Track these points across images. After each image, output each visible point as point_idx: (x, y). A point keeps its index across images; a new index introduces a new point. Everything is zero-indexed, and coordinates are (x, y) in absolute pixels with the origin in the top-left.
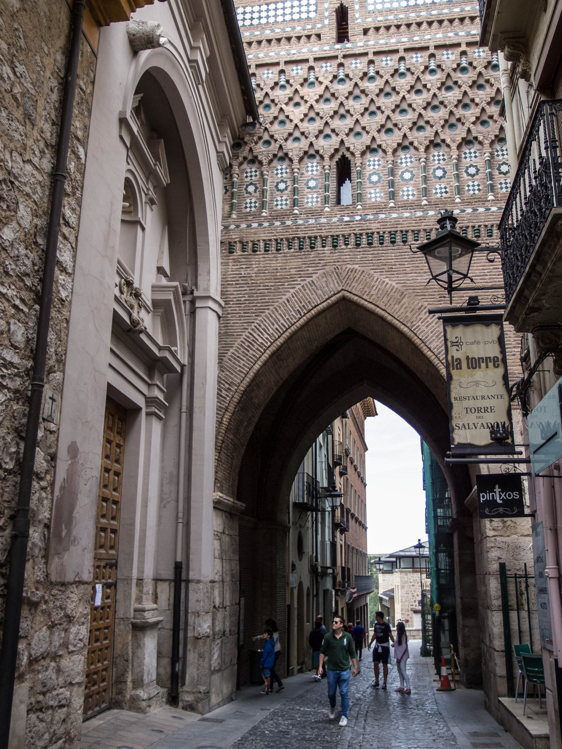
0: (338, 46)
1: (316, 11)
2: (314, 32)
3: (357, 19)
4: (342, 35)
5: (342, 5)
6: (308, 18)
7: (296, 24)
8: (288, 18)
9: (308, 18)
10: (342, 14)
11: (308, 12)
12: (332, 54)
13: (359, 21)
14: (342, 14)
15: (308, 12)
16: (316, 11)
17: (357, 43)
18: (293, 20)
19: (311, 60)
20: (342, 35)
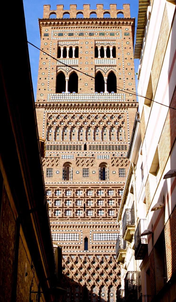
0: (85, 251)
1: (79, 238)
2: (78, 245)
3: (91, 243)
4: (86, 248)
5: (86, 237)
6: (76, 240)
7: (73, 242)
8: (70, 239)
9: (76, 240)
10: (86, 240)
12: (83, 253)
13: (91, 243)
14: (86, 240)
15: (76, 238)
16: (79, 238)
17: (90, 251)
18: (72, 240)
19: (77, 255)
20: (86, 248)
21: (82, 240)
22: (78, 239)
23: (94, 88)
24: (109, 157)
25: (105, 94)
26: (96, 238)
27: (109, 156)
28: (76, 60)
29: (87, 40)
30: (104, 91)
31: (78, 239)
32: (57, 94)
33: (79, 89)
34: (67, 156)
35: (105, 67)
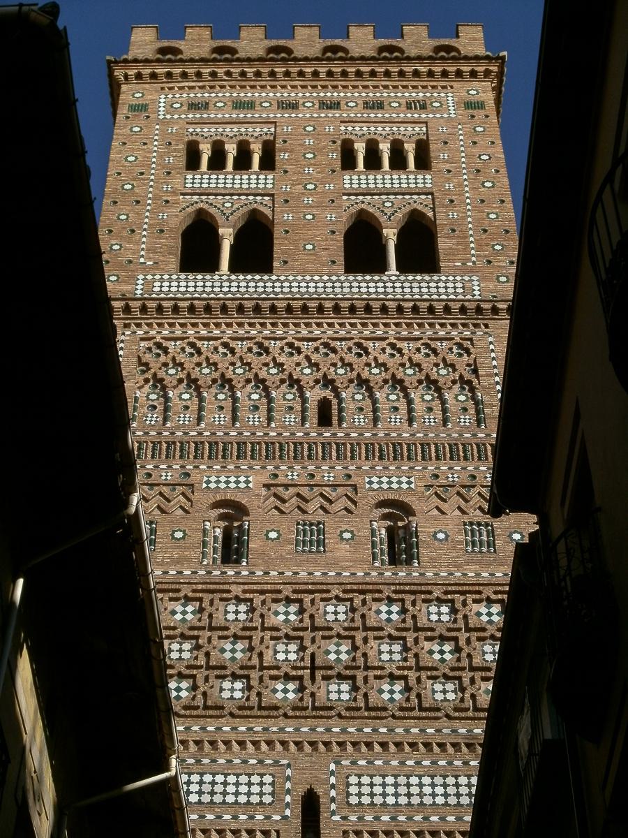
11: (261, 794)
13: (336, 818)
15: (261, 794)
21: (288, 799)
22: (267, 799)
23: (341, 261)
24: (409, 483)
25: (385, 278)
26: (360, 795)
27: (412, 480)
28: (262, 177)
29: (311, 118)
30: (381, 267)
31: (267, 799)
32: (183, 276)
33: (276, 264)
34: (220, 480)
35: (384, 197)
